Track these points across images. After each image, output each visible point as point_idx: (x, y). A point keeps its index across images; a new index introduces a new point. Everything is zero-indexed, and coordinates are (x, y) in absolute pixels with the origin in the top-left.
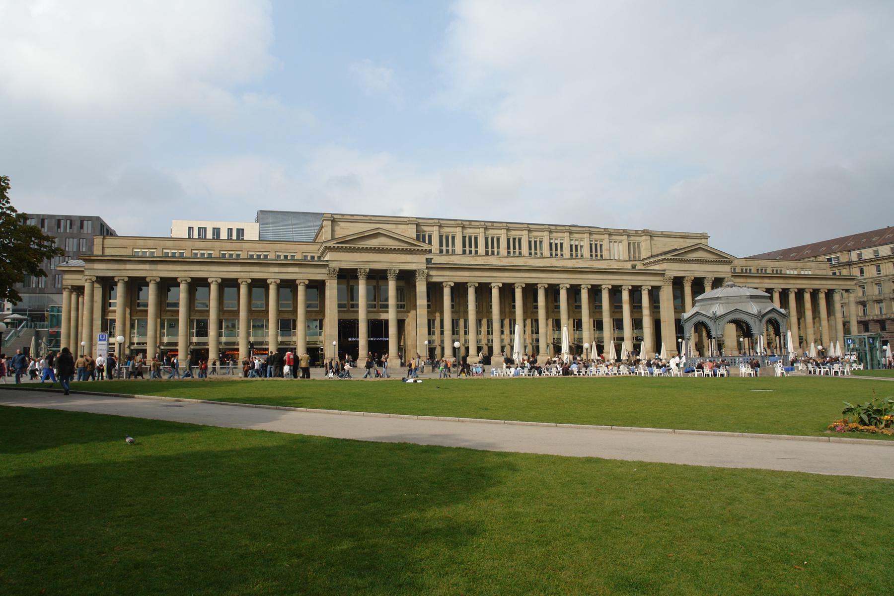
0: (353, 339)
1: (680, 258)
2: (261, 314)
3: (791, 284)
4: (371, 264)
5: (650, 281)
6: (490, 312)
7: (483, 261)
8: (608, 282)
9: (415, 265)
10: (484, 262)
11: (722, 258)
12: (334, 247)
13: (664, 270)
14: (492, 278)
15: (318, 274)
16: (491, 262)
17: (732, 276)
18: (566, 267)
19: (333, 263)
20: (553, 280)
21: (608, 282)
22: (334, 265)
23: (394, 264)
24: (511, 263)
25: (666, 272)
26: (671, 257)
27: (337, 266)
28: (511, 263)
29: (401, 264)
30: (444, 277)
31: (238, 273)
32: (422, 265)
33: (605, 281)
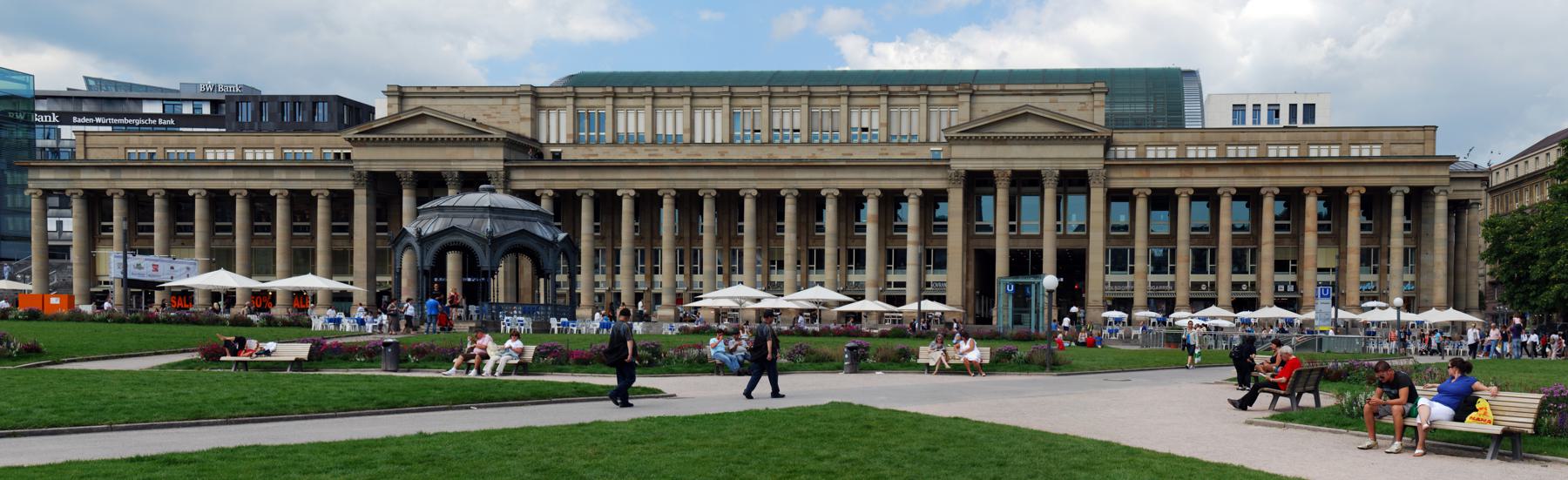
0: (441, 279)
1: (974, 135)
2: (304, 241)
3: (1264, 177)
4: (416, 163)
5: (921, 179)
6: (616, 237)
7: (648, 153)
8: (833, 184)
10: (650, 155)
11: (1083, 132)
12: (356, 139)
14: (619, 182)
15: (343, 182)
16: (662, 155)
17: (1106, 166)
18: (761, 160)
19: (361, 163)
21: (833, 184)
22: (361, 167)
24: (697, 155)
26: (959, 135)
28: (697, 155)
29: (463, 163)
30: (538, 182)
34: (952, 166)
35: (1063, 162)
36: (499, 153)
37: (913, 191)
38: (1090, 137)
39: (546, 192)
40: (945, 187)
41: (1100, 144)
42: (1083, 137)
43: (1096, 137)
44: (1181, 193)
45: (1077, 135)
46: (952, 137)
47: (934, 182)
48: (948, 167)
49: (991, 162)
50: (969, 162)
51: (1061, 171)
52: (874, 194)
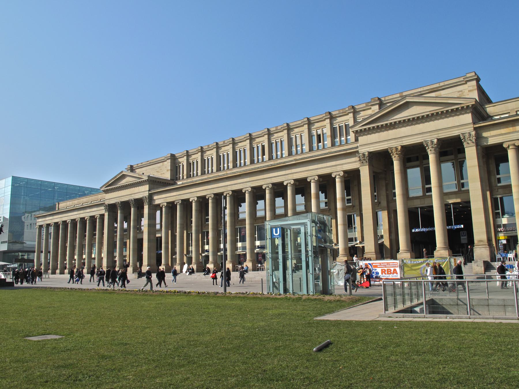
4: (122, 198)
9: (142, 193)
11: (451, 106)
13: (357, 147)
20: (236, 185)
23: (132, 195)
25: (359, 148)
27: (107, 203)
31: (76, 216)
32: (146, 193)
33: (286, 176)
34: (359, 151)
35: (439, 132)
36: (146, 187)
37: (338, 173)
38: (457, 109)
39: (164, 204)
40: (358, 167)
41: (468, 113)
42: (452, 110)
43: (462, 108)
44: (509, 147)
45: (447, 109)
46: (357, 131)
47: (351, 164)
48: (358, 152)
49: (386, 143)
50: (371, 146)
51: (438, 140)
52: (314, 179)
